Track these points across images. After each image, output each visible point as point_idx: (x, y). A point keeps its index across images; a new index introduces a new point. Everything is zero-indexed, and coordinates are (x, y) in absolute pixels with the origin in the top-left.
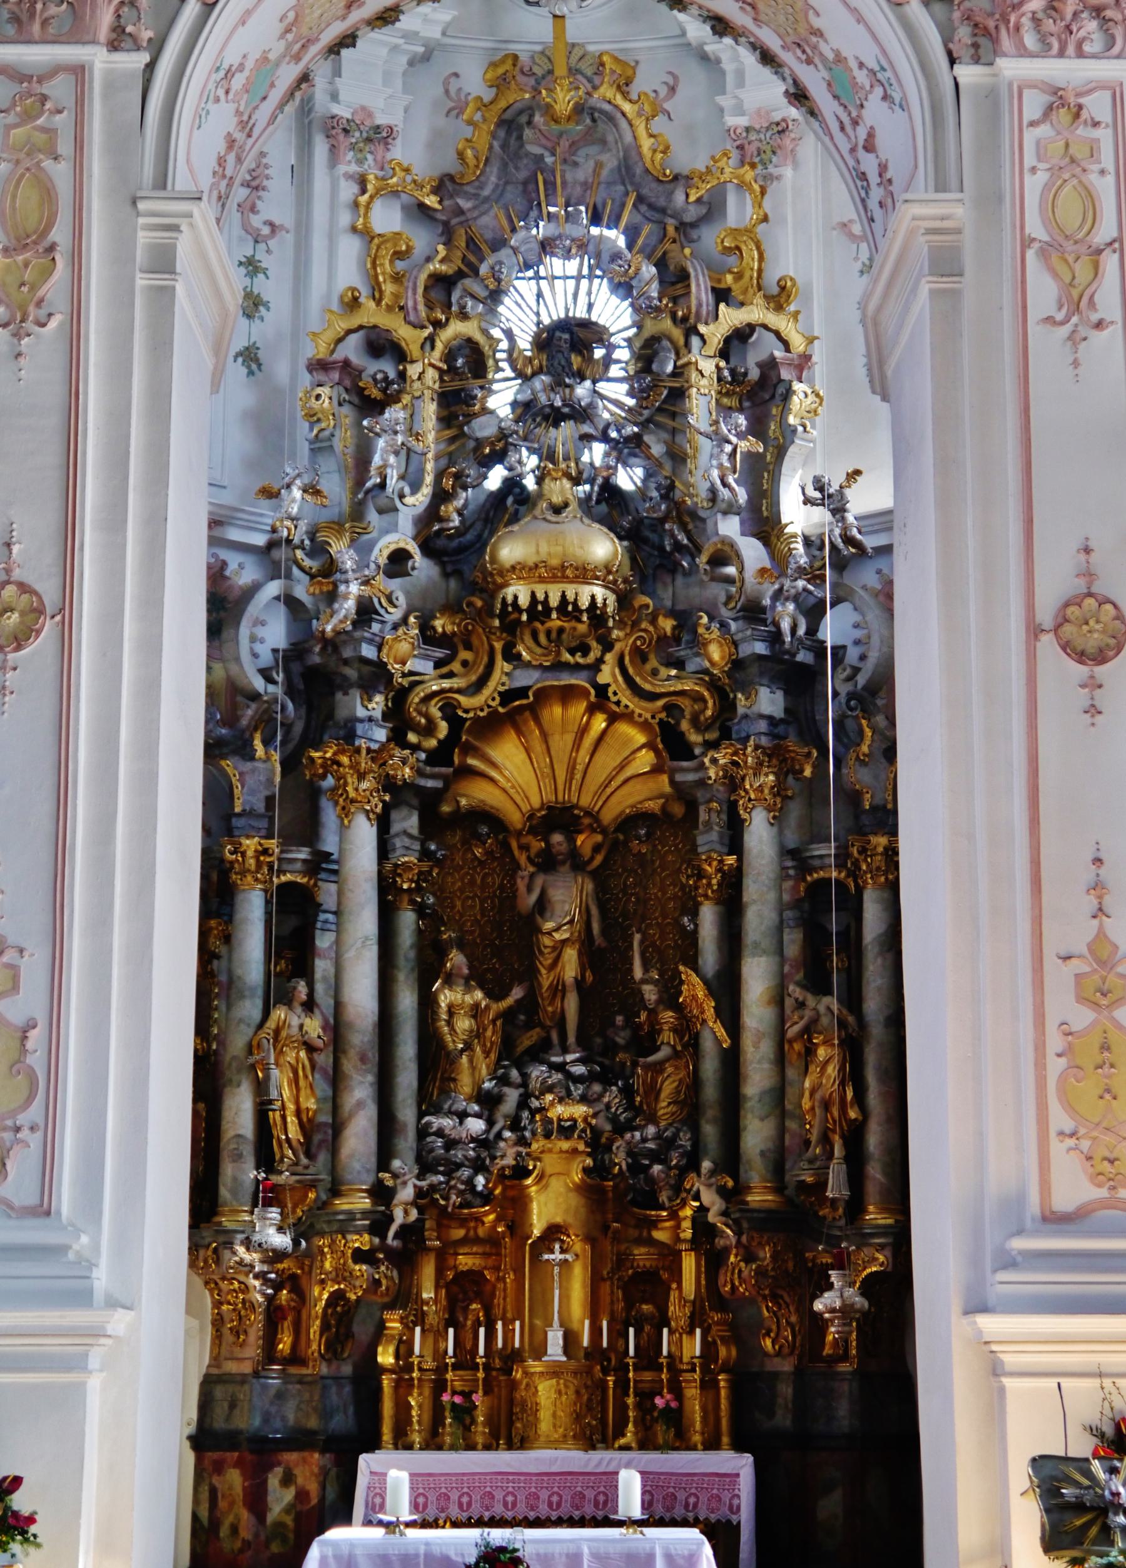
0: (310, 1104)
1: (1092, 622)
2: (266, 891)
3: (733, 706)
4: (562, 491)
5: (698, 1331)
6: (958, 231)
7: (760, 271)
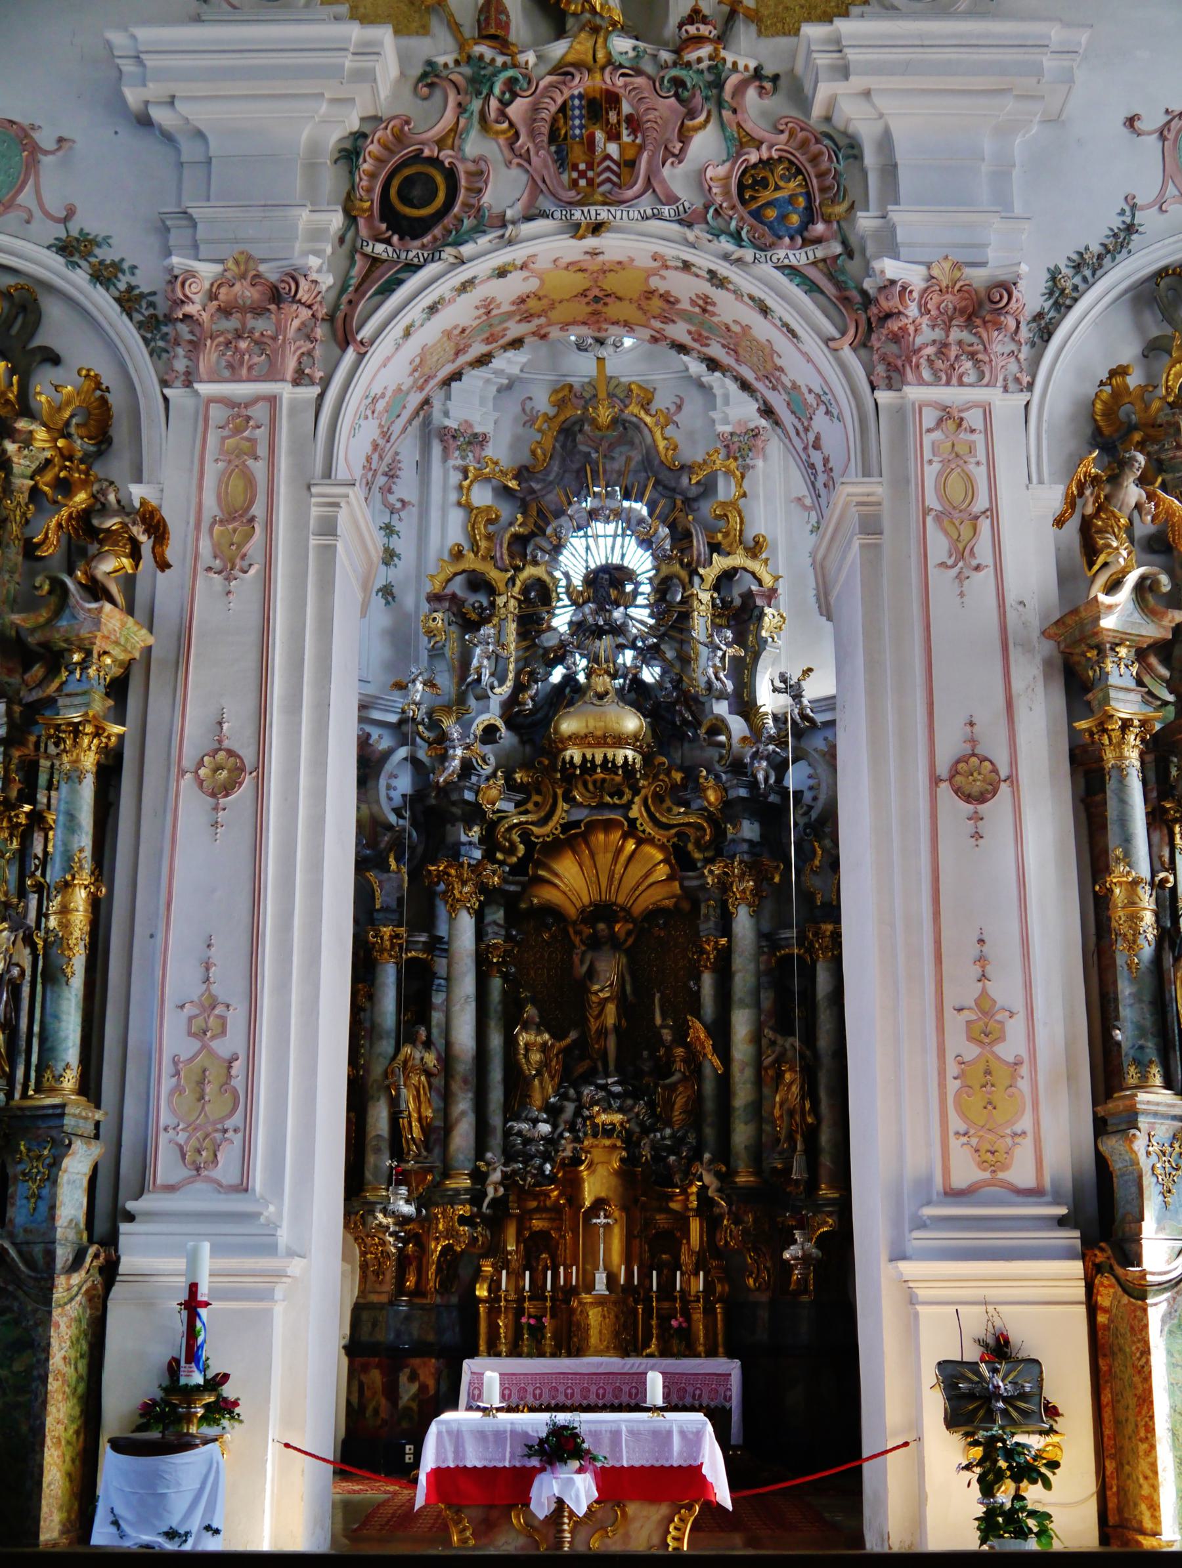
1: (975, 774)
2: (397, 963)
3: (724, 832)
4: (604, 683)
5: (701, 1273)
6: (879, 504)
7: (741, 531)
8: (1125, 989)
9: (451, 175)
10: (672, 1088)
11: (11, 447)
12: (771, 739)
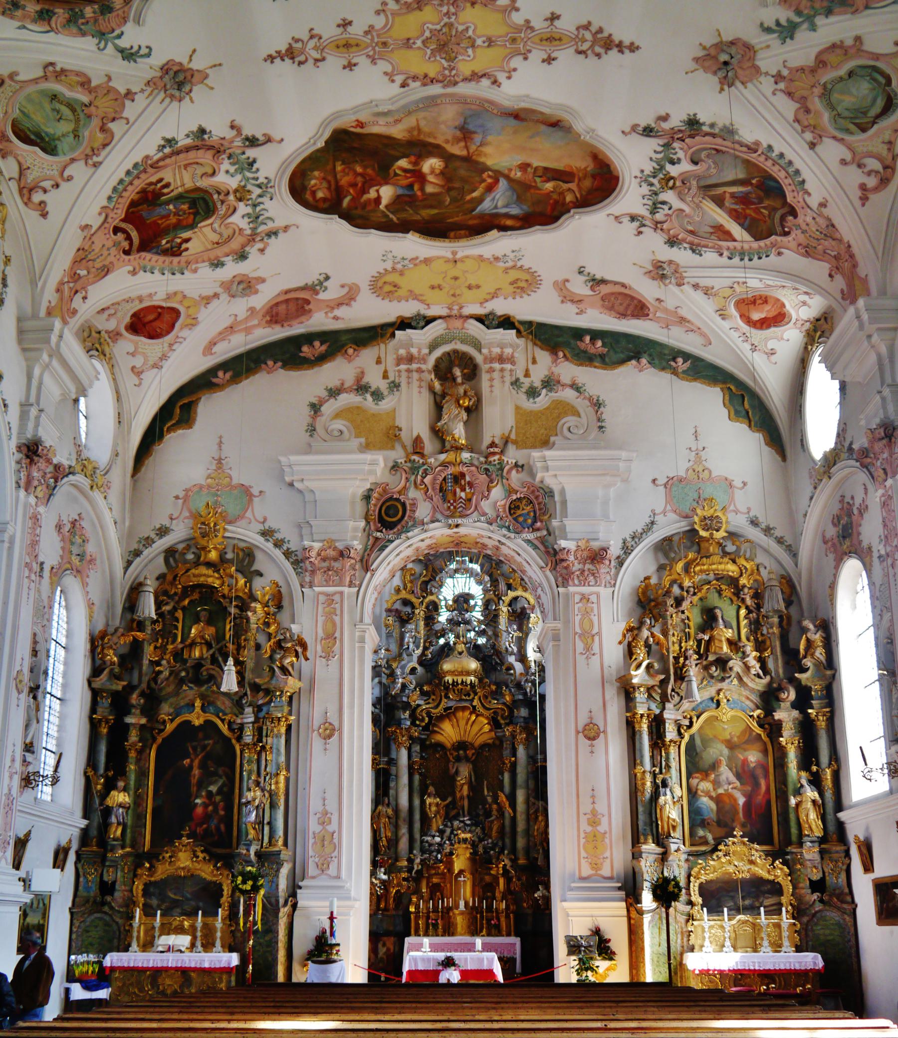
0: (389, 834)
8: (641, 809)
9: (404, 505)
10: (492, 822)
11: (250, 614)
12: (534, 674)
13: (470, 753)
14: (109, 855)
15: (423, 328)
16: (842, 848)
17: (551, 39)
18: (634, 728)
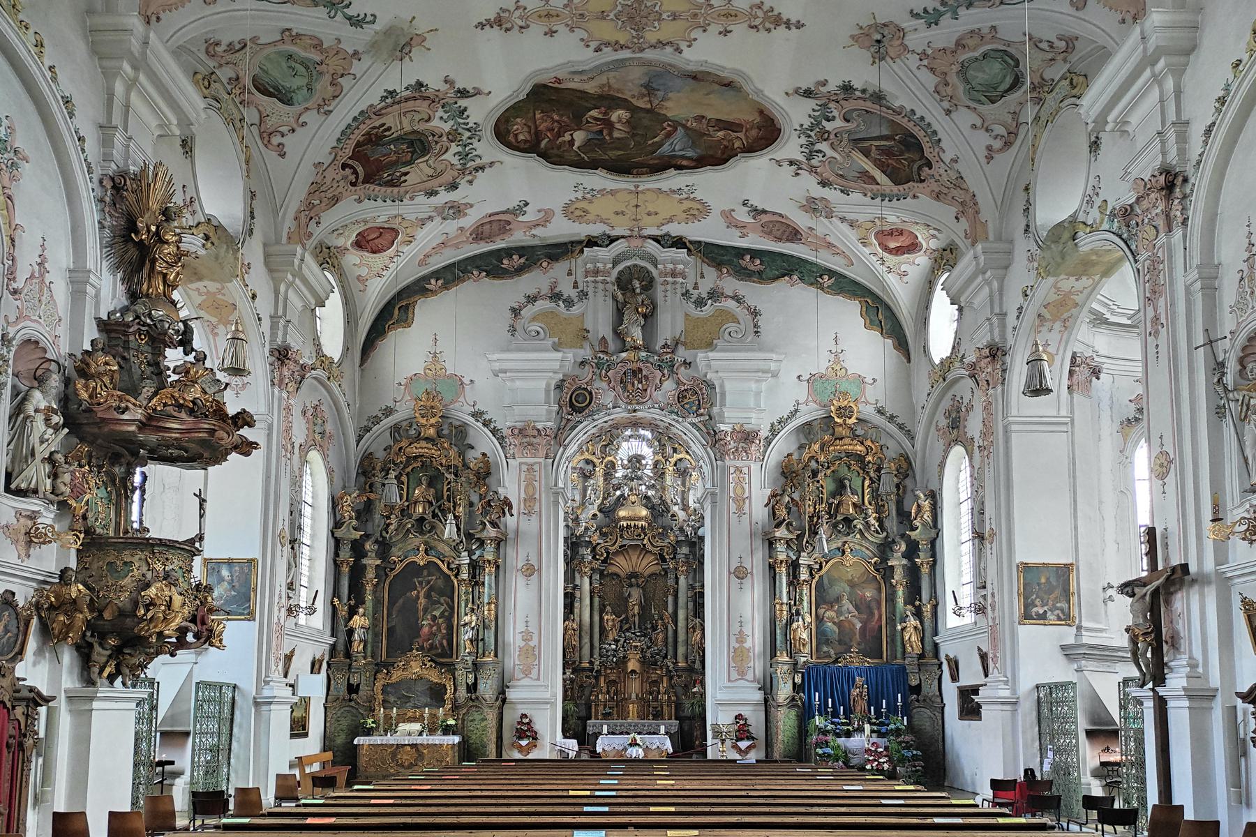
9: (590, 393)
13: (640, 581)
14: (354, 664)
15: (607, 246)
16: (935, 661)
17: (727, 15)
18: (775, 570)
